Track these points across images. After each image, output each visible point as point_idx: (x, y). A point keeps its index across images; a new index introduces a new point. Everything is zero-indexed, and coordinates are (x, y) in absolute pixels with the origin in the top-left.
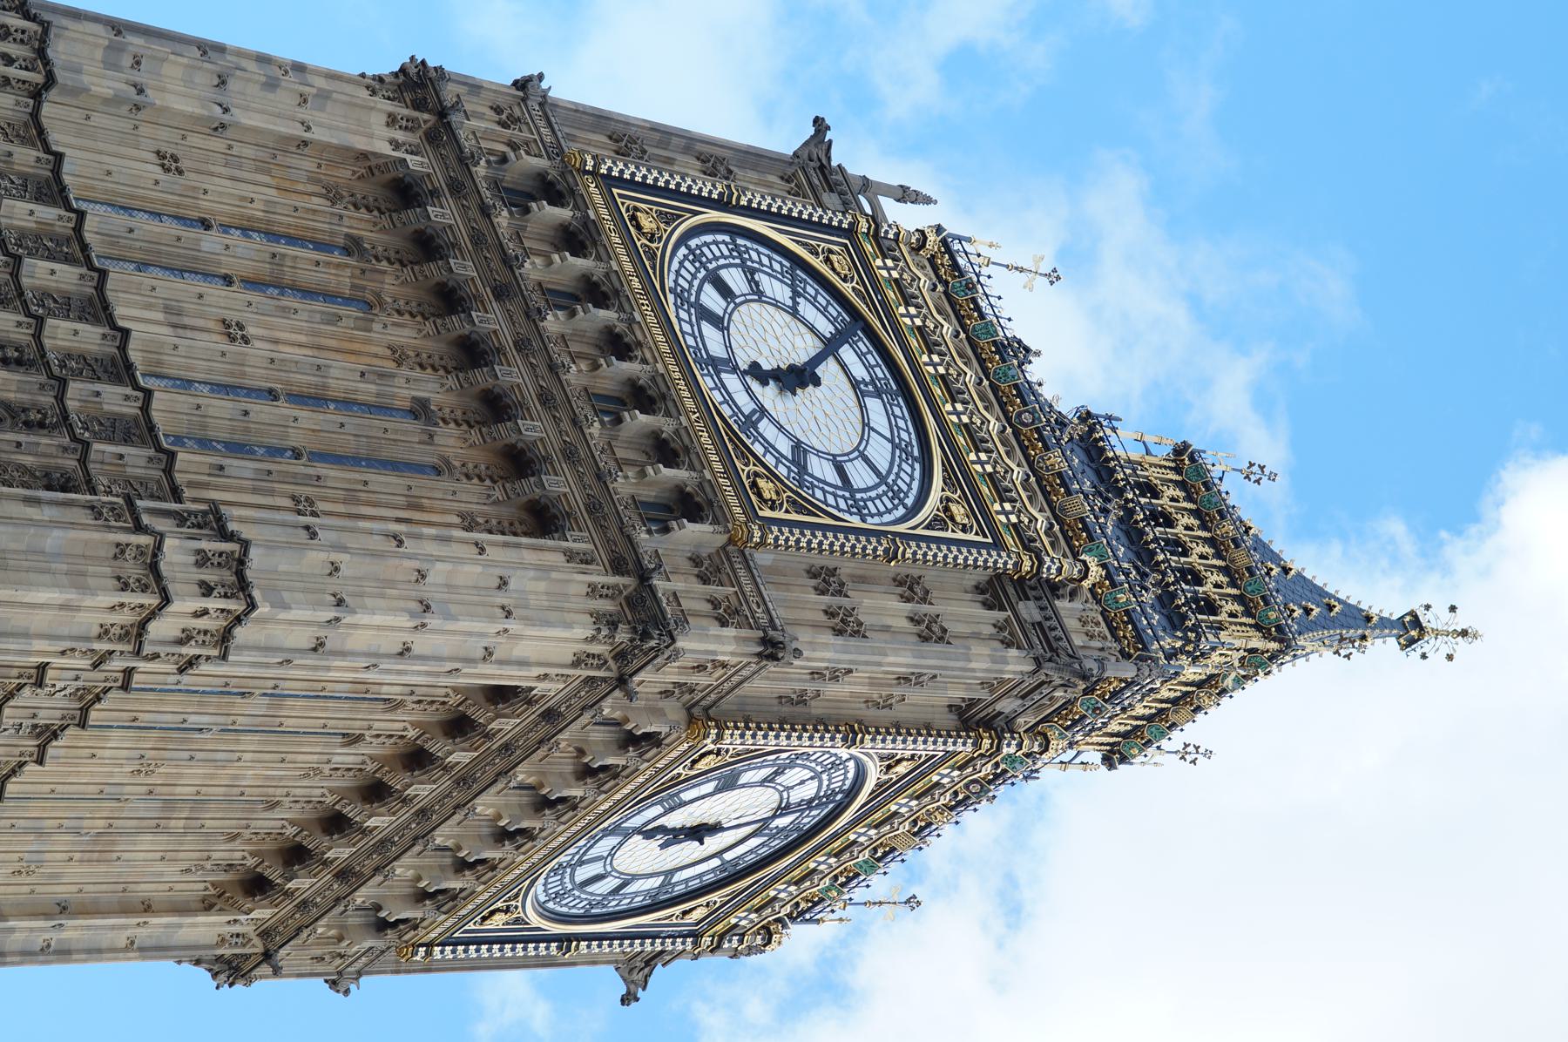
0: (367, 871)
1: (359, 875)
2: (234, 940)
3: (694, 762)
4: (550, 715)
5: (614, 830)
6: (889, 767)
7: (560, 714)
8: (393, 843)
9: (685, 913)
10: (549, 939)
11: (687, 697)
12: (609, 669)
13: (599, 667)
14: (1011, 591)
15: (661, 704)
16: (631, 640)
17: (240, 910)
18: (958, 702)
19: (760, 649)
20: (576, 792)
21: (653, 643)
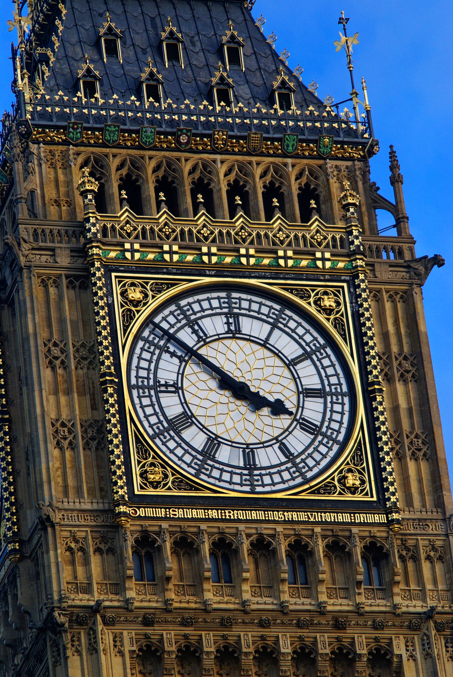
0: (329, 617)
1: (336, 619)
2: (426, 646)
3: (155, 484)
4: (148, 622)
5: (250, 465)
6: (136, 303)
7: (144, 618)
8: (299, 621)
9: (328, 311)
10: (369, 410)
11: (110, 535)
12: (94, 623)
13: (95, 632)
14: (8, 289)
15: (119, 552)
16: (66, 631)
17: (401, 662)
18: (77, 289)
19: (49, 530)
20: (206, 548)
21: (62, 619)
